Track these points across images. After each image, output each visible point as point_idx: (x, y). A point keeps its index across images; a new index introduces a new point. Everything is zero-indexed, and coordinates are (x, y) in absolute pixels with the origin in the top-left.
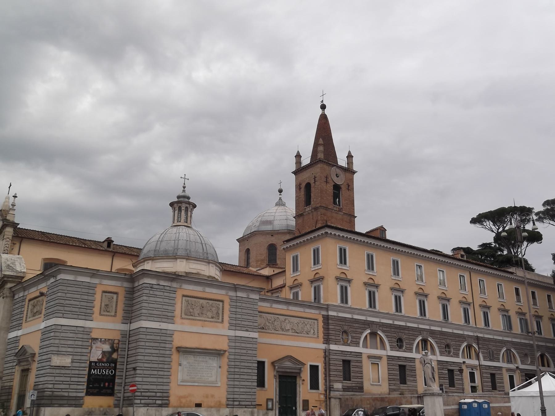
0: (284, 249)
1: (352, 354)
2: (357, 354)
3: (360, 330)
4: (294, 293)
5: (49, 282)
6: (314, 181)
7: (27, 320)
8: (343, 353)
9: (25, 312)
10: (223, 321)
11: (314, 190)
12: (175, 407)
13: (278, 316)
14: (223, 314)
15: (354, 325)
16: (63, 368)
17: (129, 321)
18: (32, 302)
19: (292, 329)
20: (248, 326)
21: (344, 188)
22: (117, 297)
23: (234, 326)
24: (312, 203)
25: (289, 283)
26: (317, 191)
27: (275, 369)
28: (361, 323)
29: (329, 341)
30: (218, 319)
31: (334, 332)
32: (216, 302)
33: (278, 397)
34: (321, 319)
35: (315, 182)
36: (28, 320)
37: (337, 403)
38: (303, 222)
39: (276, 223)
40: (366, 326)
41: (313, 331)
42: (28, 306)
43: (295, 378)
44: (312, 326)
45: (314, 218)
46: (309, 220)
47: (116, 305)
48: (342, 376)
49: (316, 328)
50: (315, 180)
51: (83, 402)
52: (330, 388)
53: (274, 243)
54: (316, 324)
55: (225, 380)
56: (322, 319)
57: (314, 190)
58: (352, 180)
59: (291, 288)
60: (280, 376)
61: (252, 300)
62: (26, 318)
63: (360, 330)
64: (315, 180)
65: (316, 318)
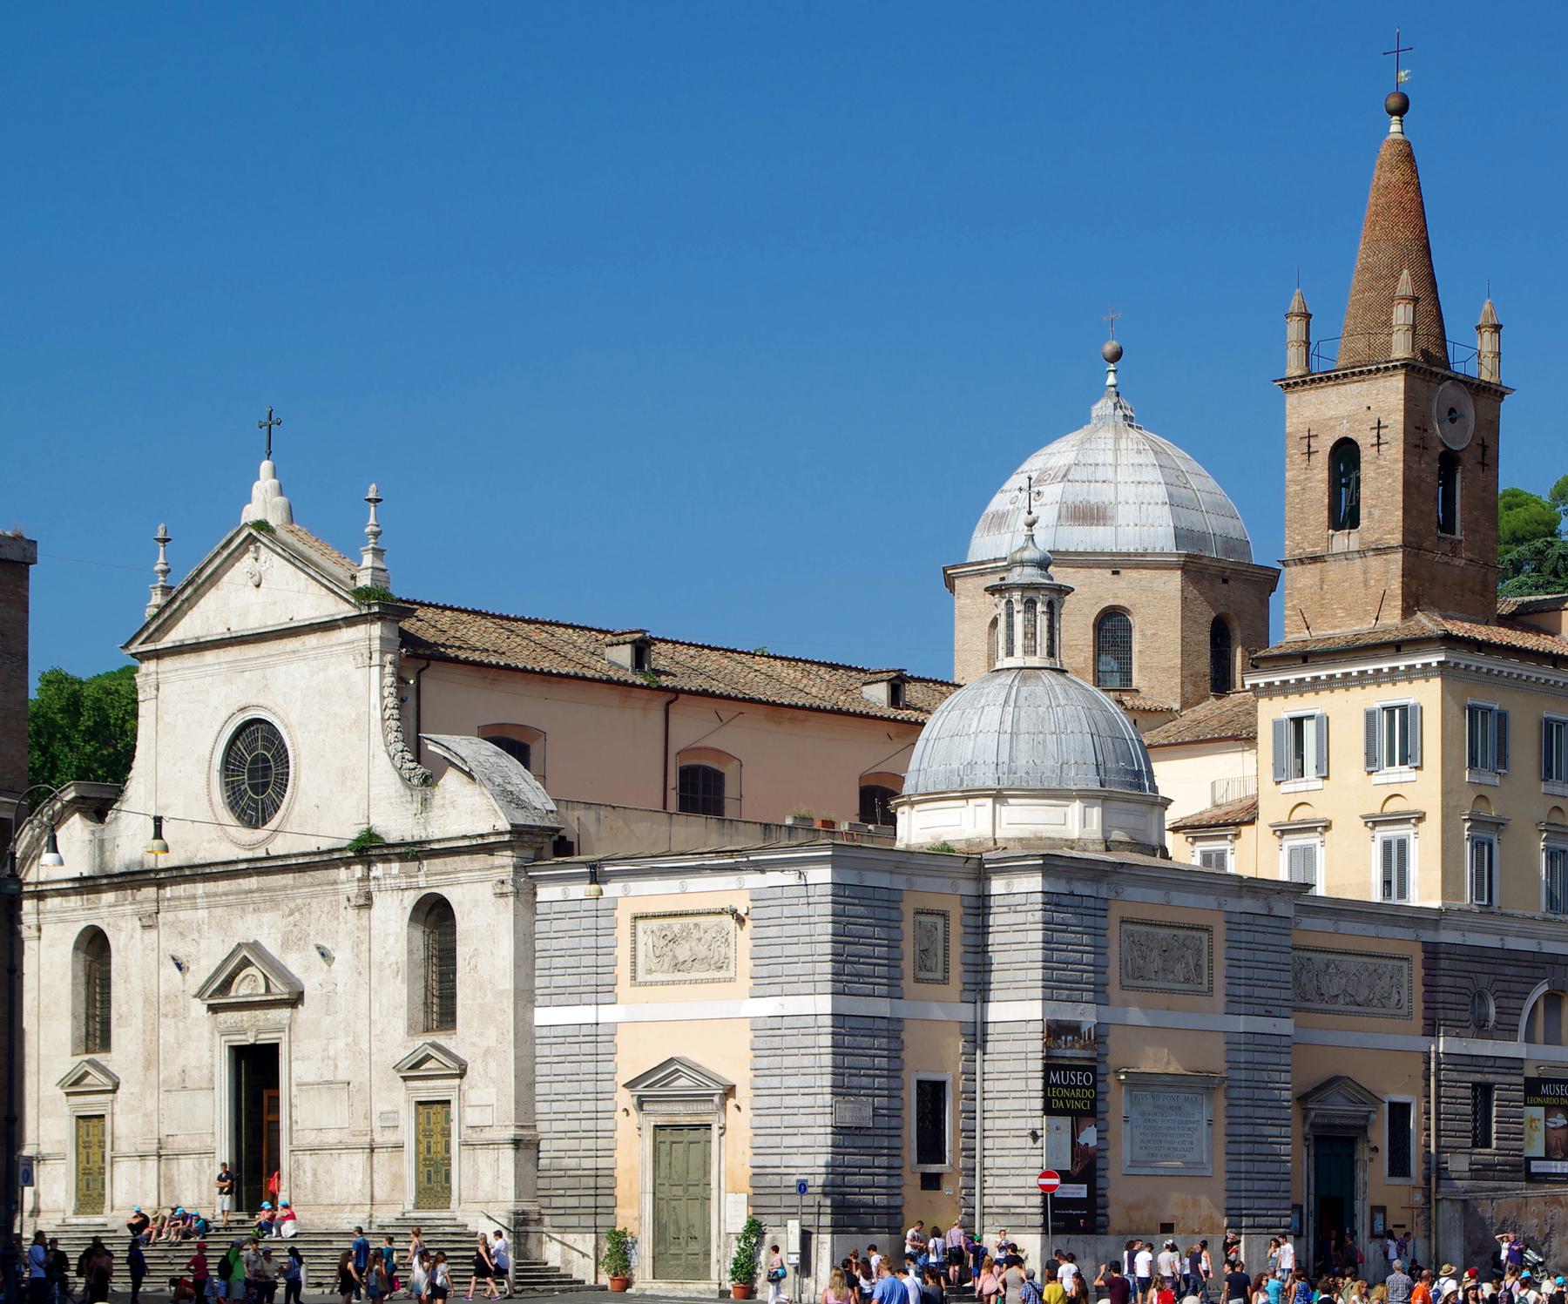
0: (1255, 686)
1: (1499, 1063)
2: (1510, 1064)
3: (1520, 987)
4: (1292, 851)
5: (753, 880)
6: (1375, 441)
7: (639, 980)
8: (1475, 1061)
9: (623, 953)
10: (1211, 989)
11: (1372, 474)
12: (1120, 1233)
13: (1309, 955)
14: (1210, 968)
15: (1507, 970)
16: (857, 1132)
17: (979, 997)
18: (655, 923)
19: (1345, 992)
20: (1270, 1002)
21: (1469, 461)
22: (946, 926)
23: (1235, 1004)
24: (1364, 522)
25: (1274, 809)
26: (1389, 481)
27: (1305, 1118)
28: (1525, 964)
29: (1440, 1025)
30: (1201, 984)
31: (1452, 998)
32: (1194, 933)
33: (1312, 1198)
34: (1418, 957)
35: (1379, 444)
36: (641, 977)
37: (1457, 1216)
38: (1322, 589)
39: (1125, 514)
40: (1539, 973)
41: (1397, 997)
42: (634, 934)
43: (1351, 1143)
44: (1395, 980)
45: (1372, 583)
46: (1347, 584)
47: (946, 949)
48: (1470, 1134)
49: (1406, 985)
50: (1379, 437)
51: (903, 1220)
52: (1438, 1169)
53: (1121, 602)
54: (1406, 971)
55: (1221, 1158)
56: (1422, 955)
57: (1372, 474)
58: (1491, 426)
59: (1283, 831)
60: (1316, 1138)
61: (1276, 922)
62: (634, 971)
63: (1520, 987)
64: (1379, 437)
65: (1405, 953)
